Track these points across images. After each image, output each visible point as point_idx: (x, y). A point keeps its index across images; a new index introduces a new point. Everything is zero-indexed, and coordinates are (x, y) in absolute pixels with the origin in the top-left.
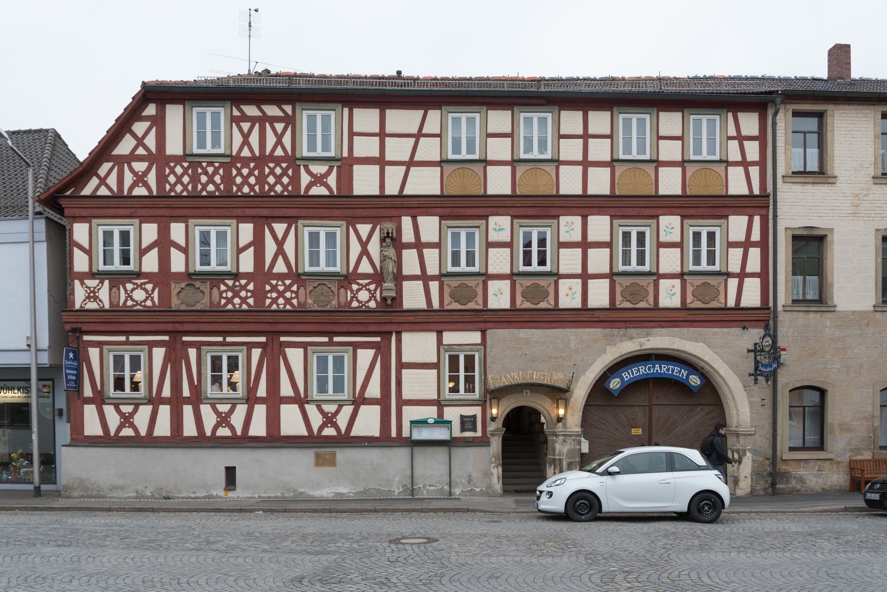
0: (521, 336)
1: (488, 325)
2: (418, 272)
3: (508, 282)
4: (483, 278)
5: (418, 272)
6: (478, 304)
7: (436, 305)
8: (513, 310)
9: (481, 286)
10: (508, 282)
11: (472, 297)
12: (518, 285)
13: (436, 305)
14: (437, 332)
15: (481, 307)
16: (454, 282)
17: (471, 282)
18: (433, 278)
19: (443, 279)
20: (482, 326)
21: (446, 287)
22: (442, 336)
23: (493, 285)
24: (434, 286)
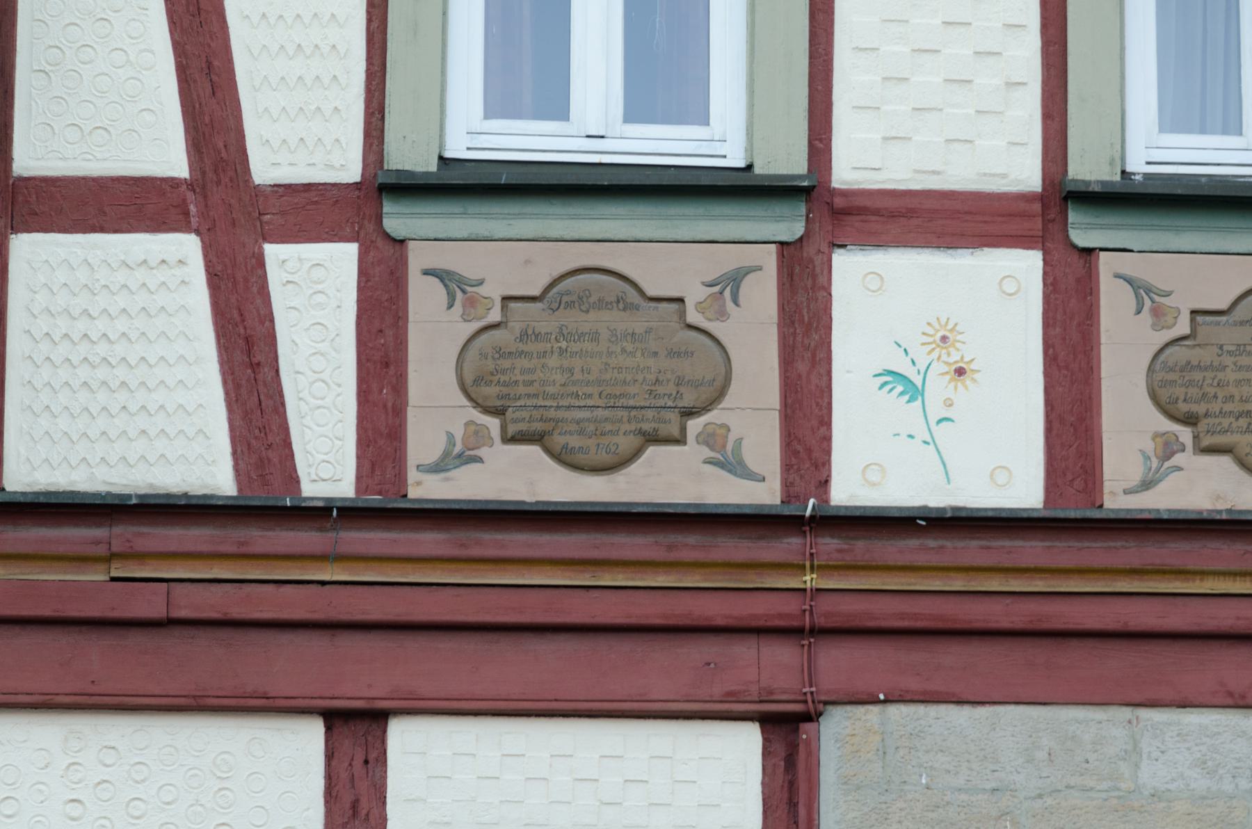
0: (1153, 774)
1: (836, 661)
2: (166, 154)
3: (1023, 268)
4: (789, 224)
5: (171, 159)
6: (734, 466)
7: (327, 463)
8: (1072, 519)
9: (763, 294)
10: (1023, 268)
11: (680, 406)
12: (1114, 303)
13: (327, 463)
14: (334, 719)
15: (765, 494)
16: (510, 255)
17: (671, 257)
18: (310, 211)
19: (399, 219)
20: (775, 668)
21: (424, 298)
22: (376, 760)
23: (873, 292)
24: (314, 286)
